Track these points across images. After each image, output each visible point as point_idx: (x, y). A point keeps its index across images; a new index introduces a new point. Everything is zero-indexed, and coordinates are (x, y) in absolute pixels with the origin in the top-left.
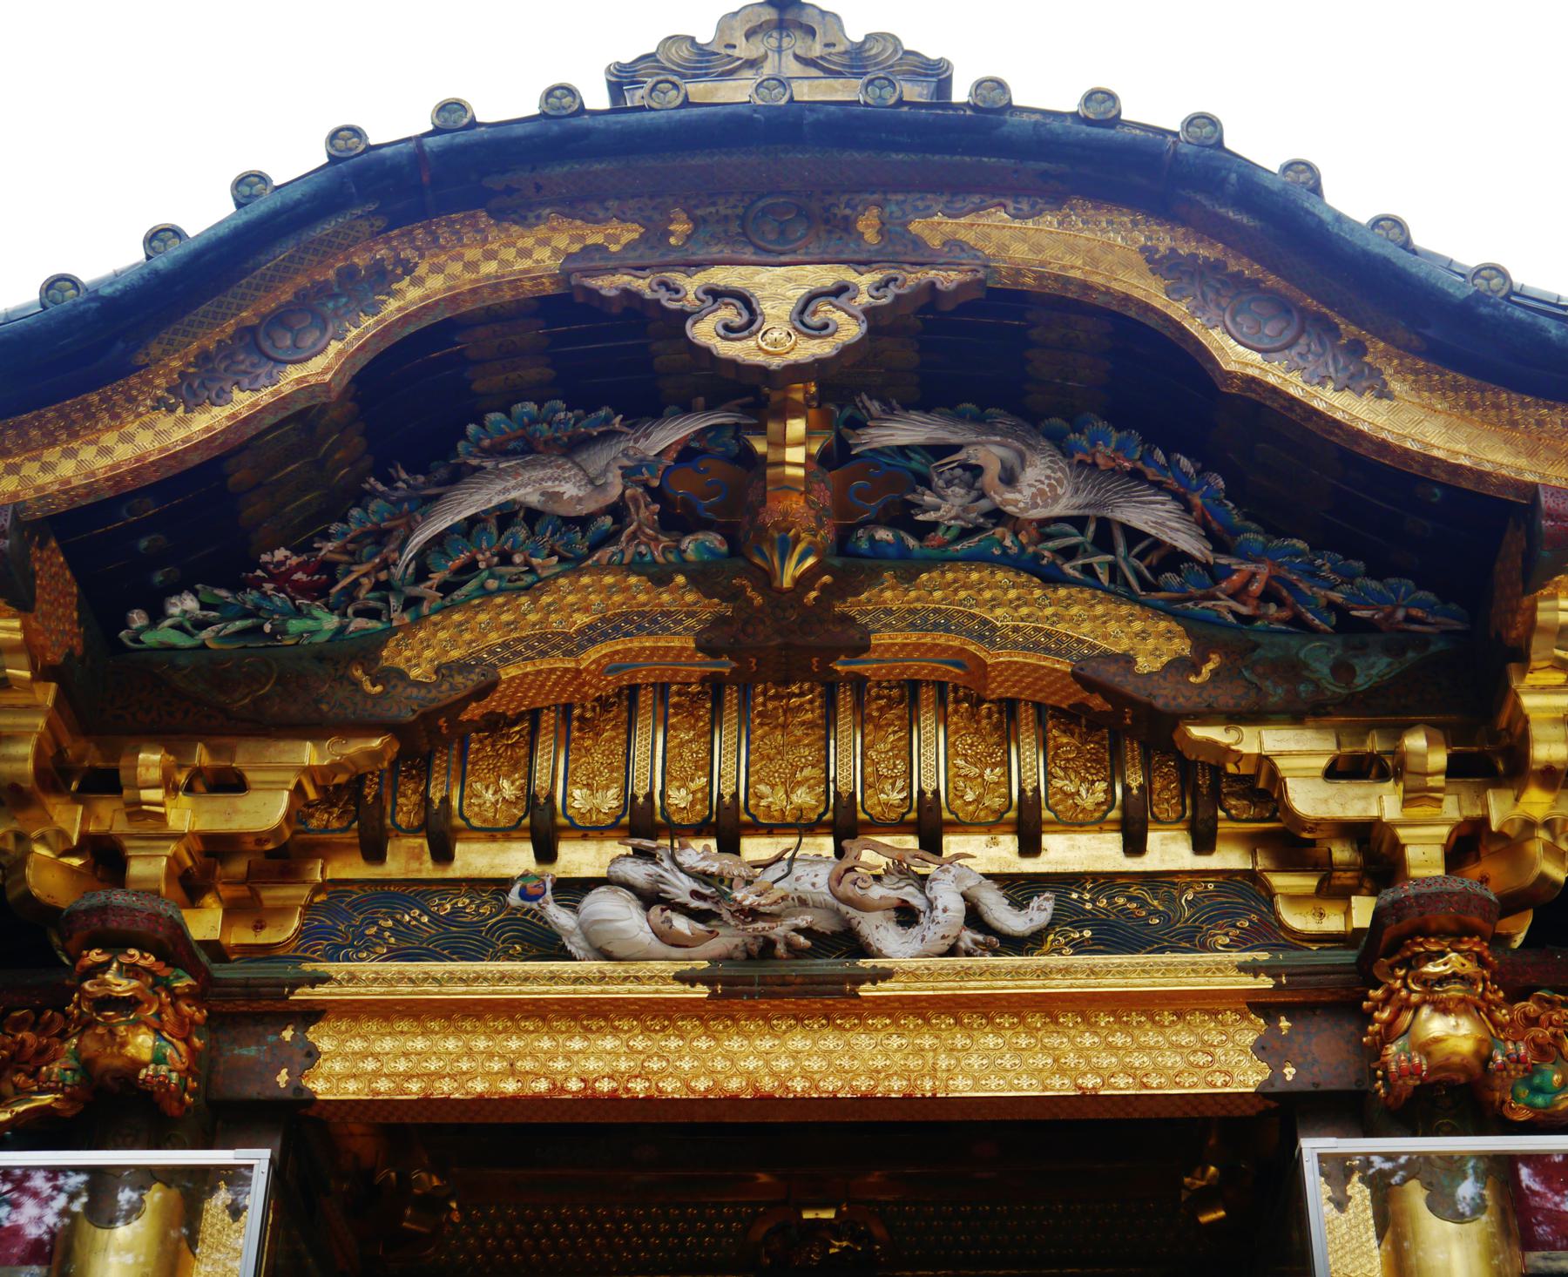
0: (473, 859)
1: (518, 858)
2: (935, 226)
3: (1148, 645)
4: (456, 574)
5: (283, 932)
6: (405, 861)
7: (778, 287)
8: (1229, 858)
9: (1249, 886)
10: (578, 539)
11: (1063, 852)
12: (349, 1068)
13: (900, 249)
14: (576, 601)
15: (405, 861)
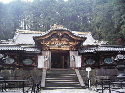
1: (54, 44)
3: (68, 40)
4: (53, 38)
6: (51, 44)
15: (51, 44)
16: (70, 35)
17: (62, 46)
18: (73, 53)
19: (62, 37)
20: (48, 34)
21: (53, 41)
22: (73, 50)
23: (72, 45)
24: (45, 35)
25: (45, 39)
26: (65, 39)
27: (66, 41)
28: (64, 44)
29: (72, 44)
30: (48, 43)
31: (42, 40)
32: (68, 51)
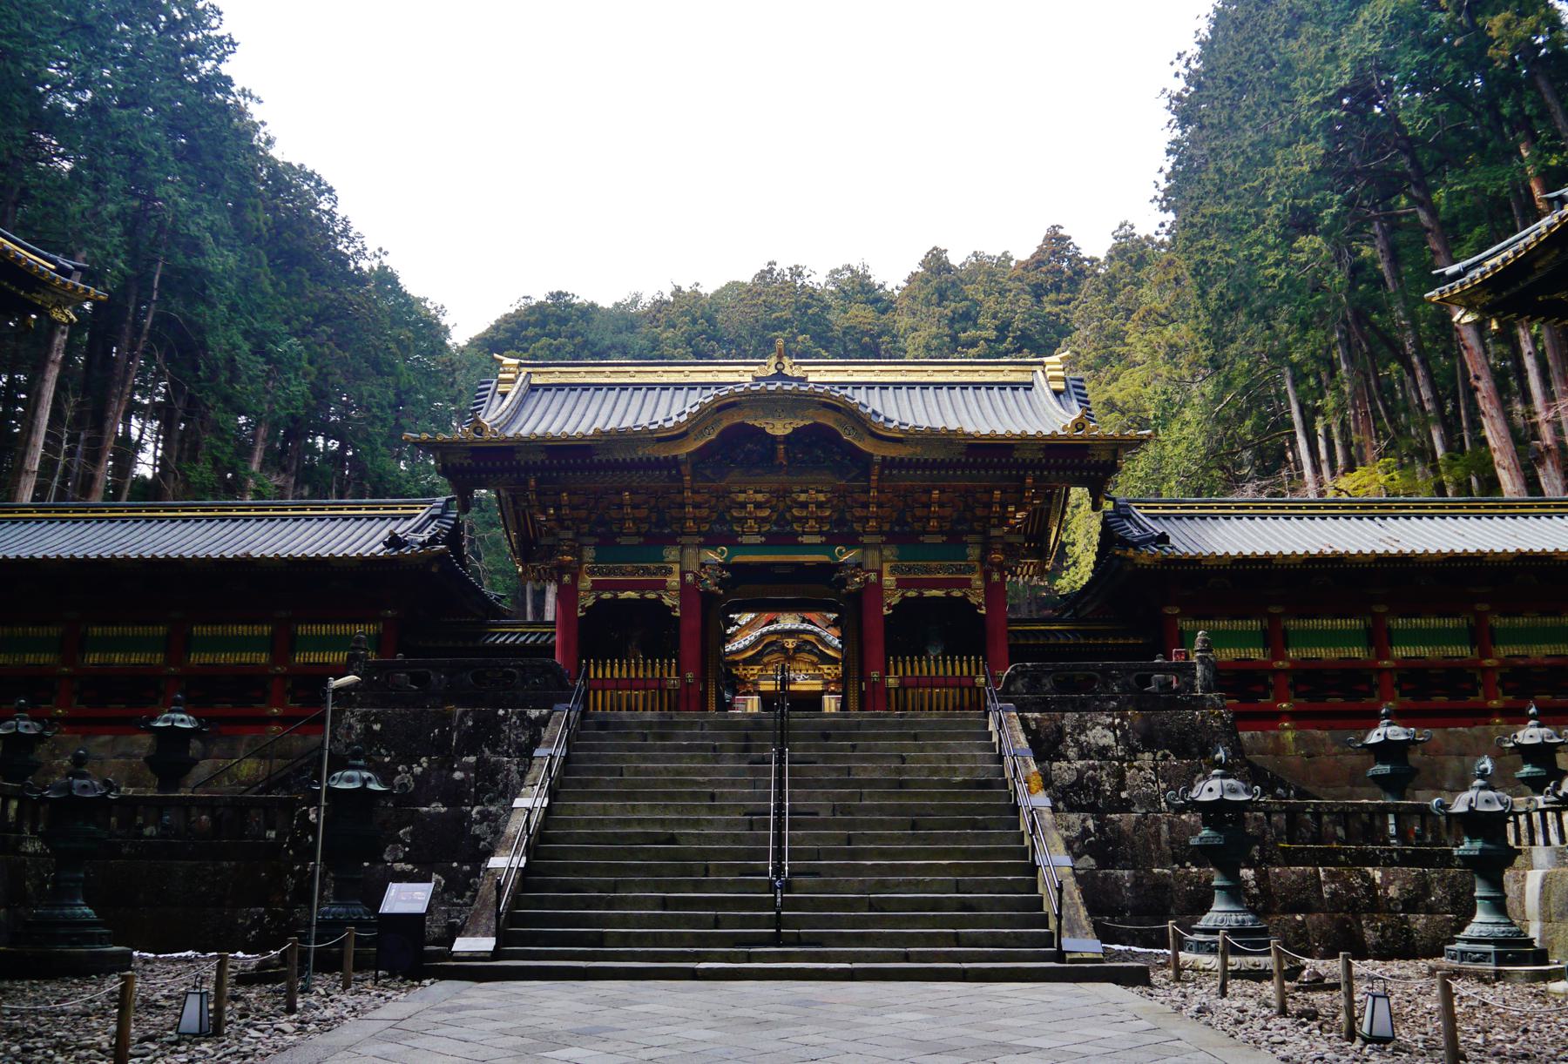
12: (762, 688)
19: (798, 649)
20: (753, 645)
21: (769, 663)
22: (832, 693)
24: (746, 649)
26: (806, 656)
27: (813, 663)
31: (736, 663)
32: (822, 693)
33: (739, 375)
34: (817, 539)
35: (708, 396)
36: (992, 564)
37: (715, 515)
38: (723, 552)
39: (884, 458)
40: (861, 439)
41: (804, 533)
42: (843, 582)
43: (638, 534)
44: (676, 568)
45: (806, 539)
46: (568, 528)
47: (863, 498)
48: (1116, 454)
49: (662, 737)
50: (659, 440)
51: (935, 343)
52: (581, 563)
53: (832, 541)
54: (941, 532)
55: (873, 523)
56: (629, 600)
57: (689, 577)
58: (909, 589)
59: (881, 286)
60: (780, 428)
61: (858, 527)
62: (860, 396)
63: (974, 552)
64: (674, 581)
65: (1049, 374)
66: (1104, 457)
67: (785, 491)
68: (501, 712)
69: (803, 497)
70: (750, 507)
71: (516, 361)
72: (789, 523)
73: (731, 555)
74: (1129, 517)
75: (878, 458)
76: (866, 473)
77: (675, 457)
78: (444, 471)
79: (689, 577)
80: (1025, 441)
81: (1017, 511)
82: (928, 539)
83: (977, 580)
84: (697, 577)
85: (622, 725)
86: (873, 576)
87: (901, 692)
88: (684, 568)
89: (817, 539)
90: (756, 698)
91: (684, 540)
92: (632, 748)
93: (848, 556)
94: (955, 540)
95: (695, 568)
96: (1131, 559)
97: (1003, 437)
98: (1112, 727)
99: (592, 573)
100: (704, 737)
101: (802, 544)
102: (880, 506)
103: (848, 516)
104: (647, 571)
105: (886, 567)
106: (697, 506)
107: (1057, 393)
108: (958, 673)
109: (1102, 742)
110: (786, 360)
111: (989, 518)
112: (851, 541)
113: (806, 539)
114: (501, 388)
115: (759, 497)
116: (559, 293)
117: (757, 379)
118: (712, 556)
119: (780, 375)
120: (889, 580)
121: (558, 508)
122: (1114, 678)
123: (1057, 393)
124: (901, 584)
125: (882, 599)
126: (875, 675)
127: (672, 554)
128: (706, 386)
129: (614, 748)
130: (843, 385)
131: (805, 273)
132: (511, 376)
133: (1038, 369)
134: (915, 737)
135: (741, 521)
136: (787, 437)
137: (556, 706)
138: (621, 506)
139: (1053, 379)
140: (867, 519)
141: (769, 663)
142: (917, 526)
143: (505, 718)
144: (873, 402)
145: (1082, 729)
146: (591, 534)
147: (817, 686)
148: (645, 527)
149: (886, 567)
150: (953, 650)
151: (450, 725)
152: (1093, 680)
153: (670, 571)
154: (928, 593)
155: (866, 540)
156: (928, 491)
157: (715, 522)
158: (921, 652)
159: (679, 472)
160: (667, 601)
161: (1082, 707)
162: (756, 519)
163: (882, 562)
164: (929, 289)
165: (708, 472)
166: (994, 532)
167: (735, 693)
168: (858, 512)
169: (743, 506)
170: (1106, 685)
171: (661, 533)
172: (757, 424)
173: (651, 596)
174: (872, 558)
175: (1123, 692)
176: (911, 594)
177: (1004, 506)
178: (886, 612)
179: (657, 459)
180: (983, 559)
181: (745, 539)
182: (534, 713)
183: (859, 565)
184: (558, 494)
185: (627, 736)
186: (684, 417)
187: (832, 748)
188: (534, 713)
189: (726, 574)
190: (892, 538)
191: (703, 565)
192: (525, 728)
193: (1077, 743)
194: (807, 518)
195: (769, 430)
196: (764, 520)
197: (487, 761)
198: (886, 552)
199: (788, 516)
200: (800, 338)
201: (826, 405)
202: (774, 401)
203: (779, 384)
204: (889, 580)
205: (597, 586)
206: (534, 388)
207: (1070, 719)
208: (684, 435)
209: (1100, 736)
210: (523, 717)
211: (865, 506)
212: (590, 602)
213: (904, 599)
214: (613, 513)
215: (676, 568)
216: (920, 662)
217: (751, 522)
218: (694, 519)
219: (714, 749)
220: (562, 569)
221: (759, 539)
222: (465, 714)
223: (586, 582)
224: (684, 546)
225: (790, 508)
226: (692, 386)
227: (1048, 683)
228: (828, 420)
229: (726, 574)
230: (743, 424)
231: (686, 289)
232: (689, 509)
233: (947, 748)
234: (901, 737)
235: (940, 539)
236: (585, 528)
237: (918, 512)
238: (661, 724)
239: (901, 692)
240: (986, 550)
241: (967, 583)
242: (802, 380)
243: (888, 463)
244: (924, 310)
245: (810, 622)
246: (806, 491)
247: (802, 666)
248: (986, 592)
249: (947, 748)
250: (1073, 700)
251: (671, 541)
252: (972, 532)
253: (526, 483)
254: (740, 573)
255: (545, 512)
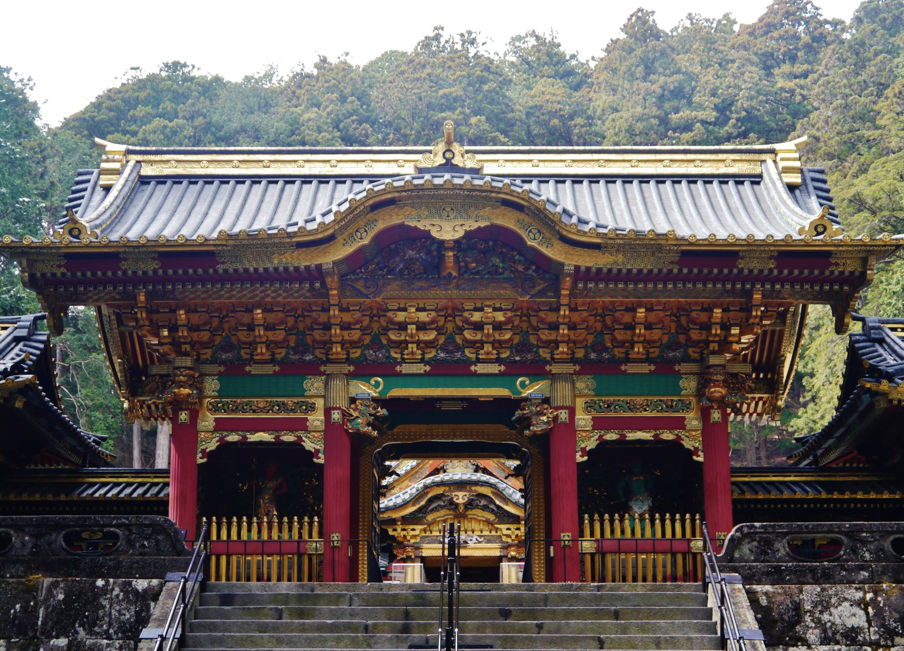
0: (434, 534)
2: (473, 488)
3: (492, 517)
4: (432, 510)
5: (418, 540)
6: (428, 534)
7: (461, 494)
8: (499, 534)
9: (500, 536)
10: (442, 507)
11: (484, 533)
12: (425, 553)
13: (471, 491)
14: (443, 512)
15: (428, 534)
16: (498, 502)
17: (471, 544)
18: (513, 570)
19: (469, 505)
21: (434, 522)
22: (513, 559)
23: (508, 536)
24: (405, 504)
25: (403, 517)
26: (478, 513)
27: (488, 522)
28: (479, 533)
29: (508, 532)
30: (413, 530)
31: (393, 522)
32: (500, 559)
33: (400, 166)
34: (494, 369)
35: (360, 191)
36: (711, 400)
37: (367, 340)
38: (377, 384)
39: (577, 268)
40: (550, 245)
41: (478, 361)
42: (526, 422)
43: (273, 361)
44: (320, 403)
45: (480, 368)
46: (186, 354)
47: (552, 317)
48: (865, 262)
49: (301, 614)
50: (300, 245)
51: (639, 126)
52: (201, 396)
53: (513, 370)
54: (648, 360)
55: (563, 348)
56: (261, 443)
57: (336, 416)
58: (608, 429)
59: (573, 57)
60: (448, 230)
61: (544, 353)
62: (548, 191)
63: (689, 385)
64: (316, 419)
65: (782, 164)
66: (851, 266)
67: (455, 308)
68: (100, 583)
69: (477, 317)
70: (412, 328)
71: (123, 148)
72: (460, 349)
73: (387, 388)
74: (881, 341)
75: (569, 268)
76: (555, 285)
77: (319, 267)
78: (32, 282)
79: (336, 416)
80: (752, 246)
81: (742, 333)
82: (631, 368)
83: (693, 420)
84: (345, 414)
85: (251, 598)
86: (563, 415)
87: (598, 558)
88: (327, 407)
89: (494, 369)
90: (418, 565)
91: (329, 369)
92: (263, 628)
93: (533, 389)
94: (665, 367)
95: (343, 403)
96: (885, 394)
97: (725, 243)
98: (862, 604)
99: (215, 409)
100: (352, 615)
101: (475, 374)
102: (572, 327)
103: (533, 340)
104: (283, 407)
105: (580, 403)
106: (346, 327)
107: (791, 188)
108: (669, 535)
109: (851, 622)
110: (457, 148)
111: (707, 343)
112: (536, 370)
113: (480, 368)
114: (104, 180)
115: (423, 317)
116: (176, 64)
117: (421, 171)
118: (365, 389)
119: (449, 166)
120: (583, 419)
121: (173, 329)
122: (864, 542)
123: (791, 188)
124: (599, 424)
125: (575, 443)
126: (566, 536)
127: (314, 385)
128: (357, 179)
129: (242, 628)
130: (527, 178)
131: (480, 40)
132: (117, 166)
133: (769, 158)
134: (616, 615)
135: (401, 345)
136: (457, 242)
137: (169, 575)
138: (251, 327)
139: (786, 170)
140: (557, 344)
141: (434, 522)
142: (618, 352)
143: (105, 590)
144: (563, 199)
145: (826, 606)
146: (213, 361)
147: (494, 550)
148: (281, 353)
149: (580, 403)
150: (662, 506)
151: (35, 598)
152: (837, 544)
153: (312, 408)
154: (631, 436)
155: (555, 369)
156: (632, 309)
157: (368, 347)
158: (620, 507)
159: (323, 284)
160: (309, 445)
161: (825, 578)
162: (418, 343)
163: (575, 396)
164: (632, 60)
165: (360, 285)
166: (714, 360)
167: (392, 558)
168: (546, 335)
169: (402, 327)
170: (854, 551)
171: (301, 361)
172: (420, 226)
173: (288, 438)
174: (562, 393)
175: (877, 559)
176: (611, 436)
177: (726, 327)
178: (580, 458)
179: (297, 269)
180: (700, 393)
181: (405, 369)
182: (141, 584)
183: (546, 401)
184: (173, 311)
185: (257, 612)
186: (330, 218)
187: (512, 629)
188: (141, 584)
189: (382, 412)
190: (587, 367)
191: (353, 400)
192: (129, 602)
193: (819, 623)
194: (482, 343)
195: (435, 234)
196: (429, 344)
197: (81, 644)
198: (580, 385)
199: (458, 340)
200: (474, 120)
201: (506, 203)
202: (441, 198)
203: (447, 176)
204: (583, 419)
205: (221, 426)
206: (144, 181)
207: (810, 593)
208: (331, 238)
209: (847, 614)
210: (127, 588)
211: (554, 327)
212: (212, 446)
213: (602, 443)
214: (242, 336)
215: (320, 403)
216: (622, 521)
217: (412, 347)
218: (343, 343)
219: (366, 628)
220: (178, 404)
221: (422, 368)
222: (55, 585)
223: (207, 421)
224: (329, 377)
225: (460, 330)
226: (340, 179)
227: (782, 548)
228: (508, 220)
229: (382, 412)
230: (402, 226)
231: (333, 60)
232: (336, 331)
233: (655, 629)
234: (598, 614)
235: (645, 368)
236: (207, 354)
237: (620, 335)
238: (300, 598)
239: (598, 558)
240: (704, 381)
241: (679, 423)
242: (476, 171)
243: (582, 275)
244: (627, 85)
245: (485, 471)
246: (481, 309)
247: (475, 525)
248: (703, 434)
249: (655, 629)
250: (813, 570)
251: (313, 369)
252: (686, 359)
253: (134, 297)
254: (399, 410)
255: (157, 335)
